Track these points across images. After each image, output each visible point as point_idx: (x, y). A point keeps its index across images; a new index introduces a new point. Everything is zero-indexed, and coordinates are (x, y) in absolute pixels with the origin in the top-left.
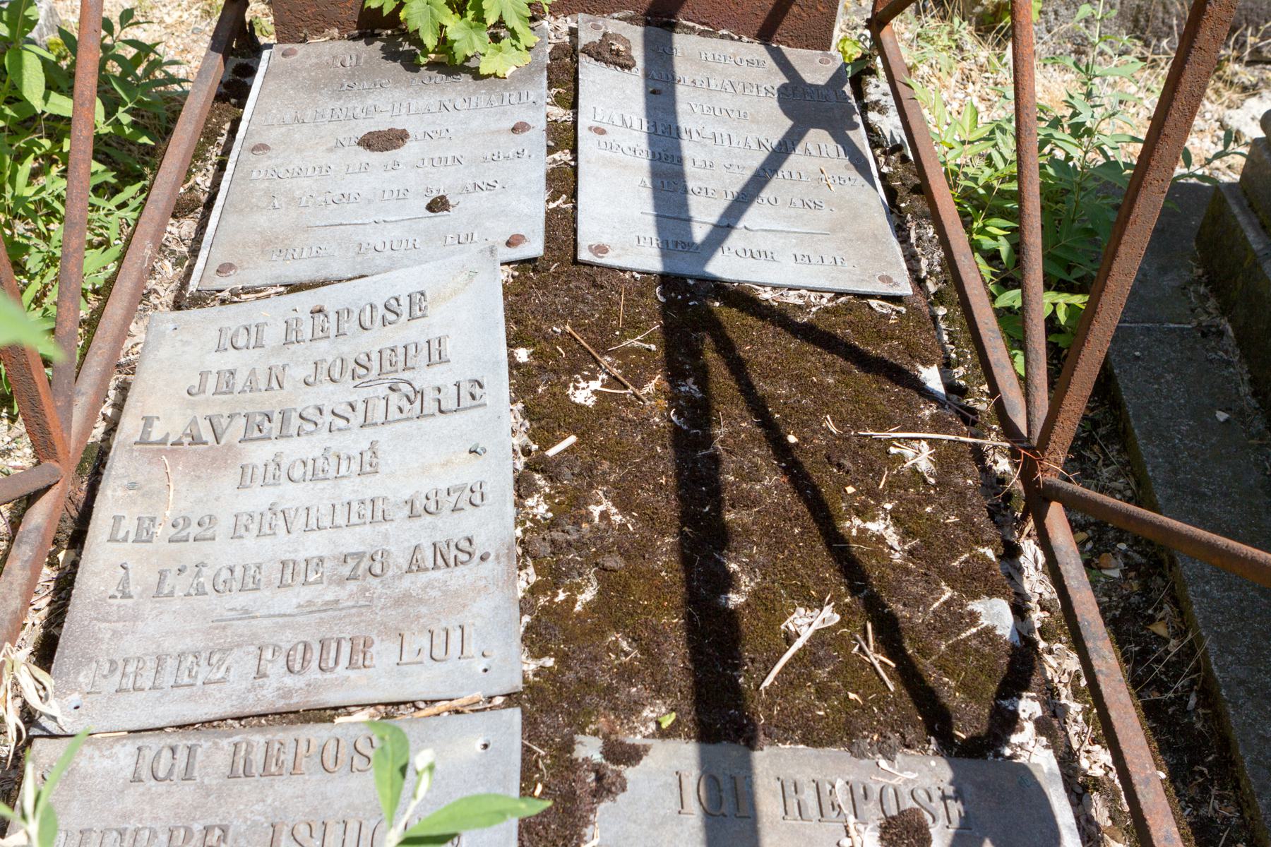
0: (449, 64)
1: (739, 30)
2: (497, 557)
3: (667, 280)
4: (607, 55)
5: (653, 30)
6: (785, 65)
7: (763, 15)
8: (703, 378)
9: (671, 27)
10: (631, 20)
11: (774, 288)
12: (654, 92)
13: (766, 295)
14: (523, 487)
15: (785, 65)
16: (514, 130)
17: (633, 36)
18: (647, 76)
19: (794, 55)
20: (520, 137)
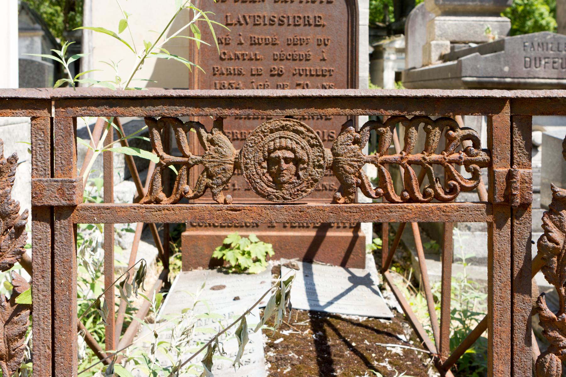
0: (240, 270)
1: (333, 263)
2: (258, 362)
3: (311, 312)
4: (290, 266)
5: (306, 263)
6: (350, 272)
7: (341, 259)
8: (324, 331)
9: (311, 262)
10: (298, 260)
11: (347, 315)
12: (306, 276)
13: (343, 317)
14: (266, 350)
15: (350, 272)
16: (261, 283)
17: (300, 264)
18: (304, 272)
19: (352, 270)
20: (263, 285)
